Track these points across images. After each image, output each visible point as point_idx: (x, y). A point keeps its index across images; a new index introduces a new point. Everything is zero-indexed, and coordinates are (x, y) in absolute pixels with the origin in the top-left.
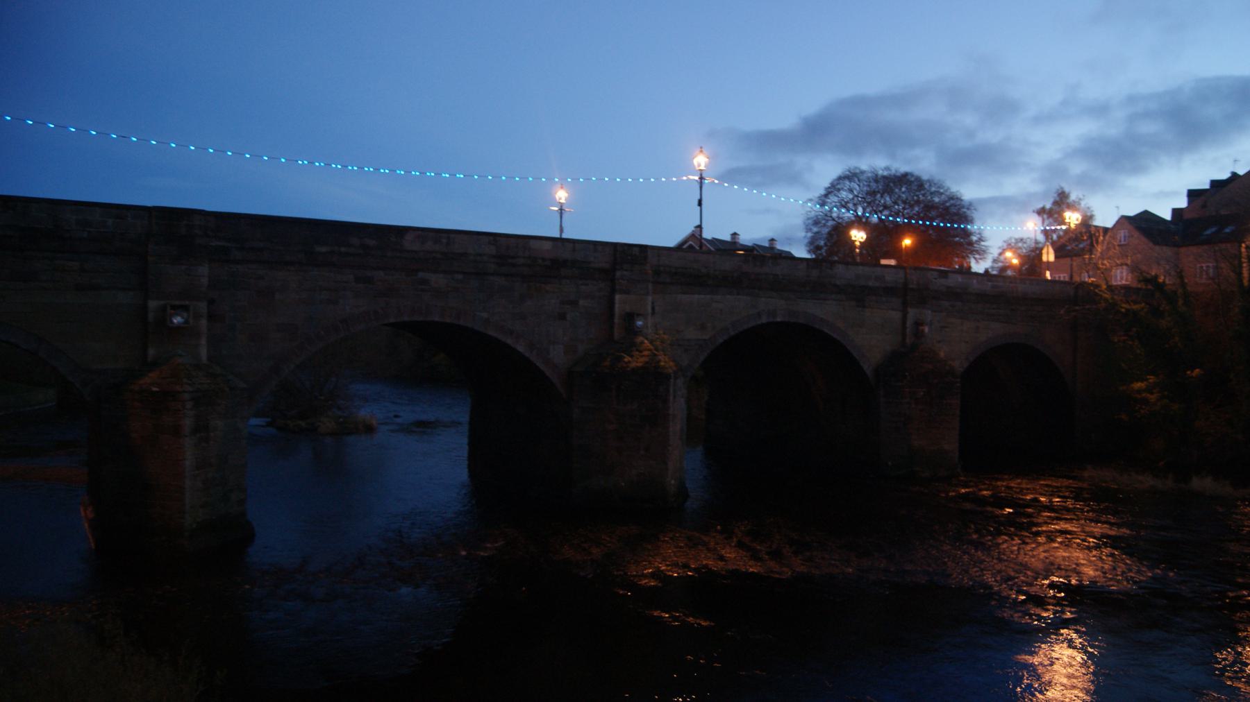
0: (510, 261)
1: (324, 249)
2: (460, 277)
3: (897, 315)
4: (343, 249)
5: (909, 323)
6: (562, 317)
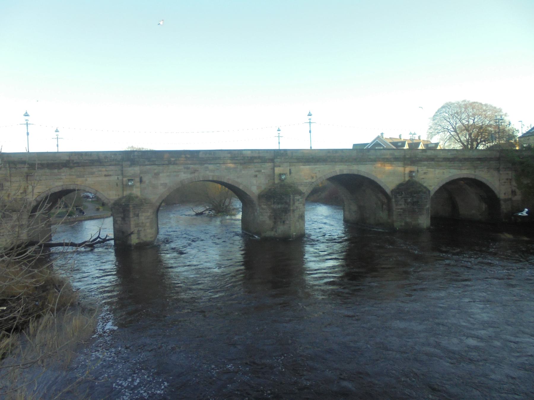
2: (219, 165)
6: (256, 176)
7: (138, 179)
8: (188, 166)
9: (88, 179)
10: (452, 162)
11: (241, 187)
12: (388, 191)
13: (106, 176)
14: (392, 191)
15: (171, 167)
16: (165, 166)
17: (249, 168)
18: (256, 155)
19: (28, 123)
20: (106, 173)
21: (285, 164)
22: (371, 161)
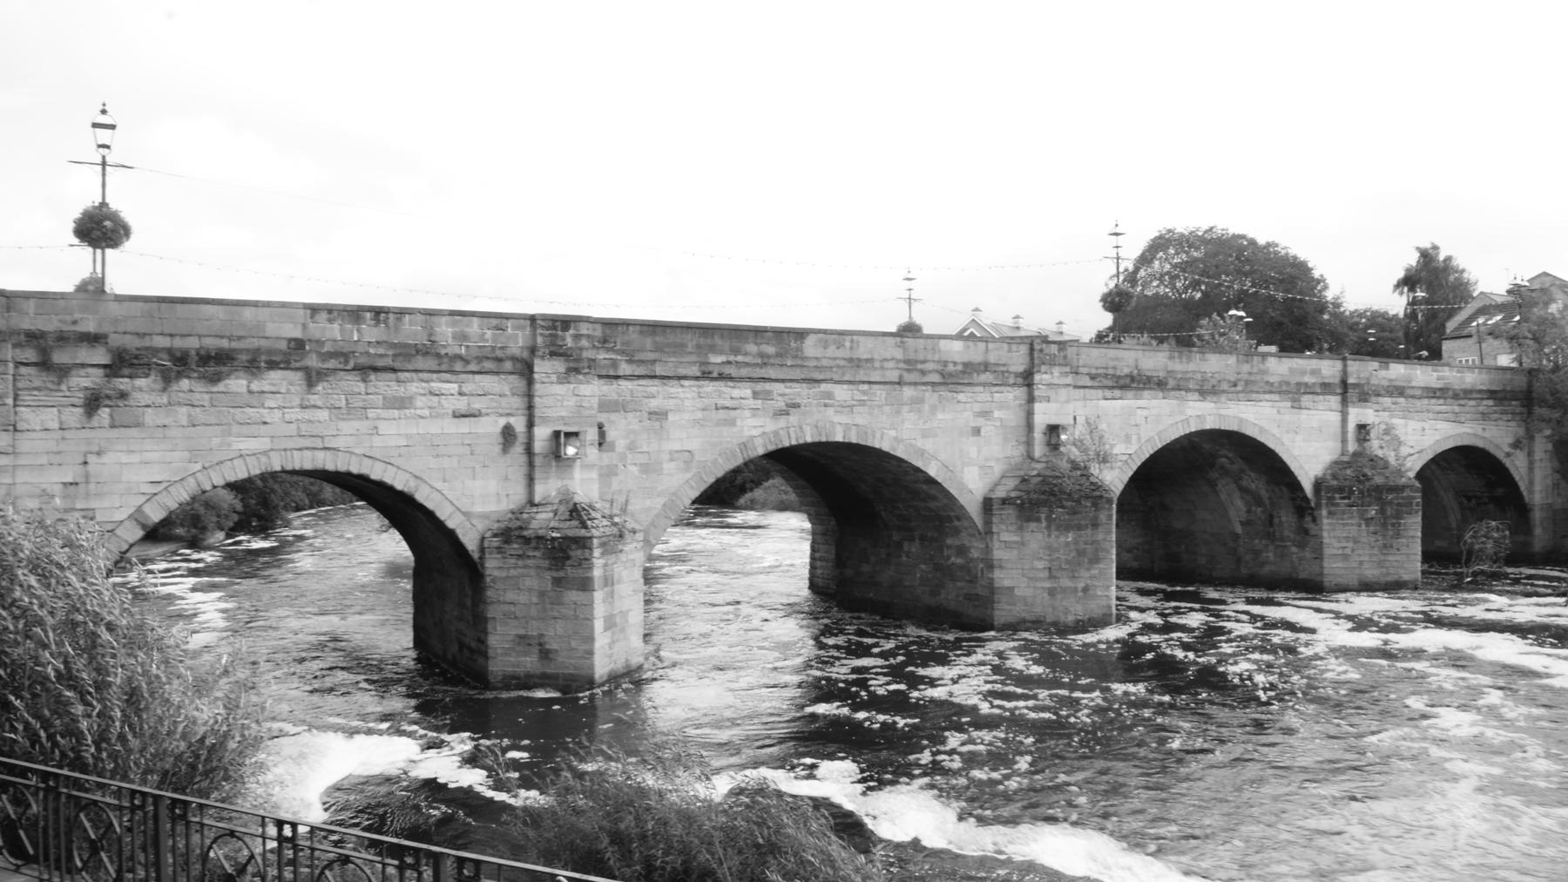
0: (920, 366)
2: (866, 387)
3: (1335, 417)
4: (740, 358)
5: (1351, 426)
6: (977, 431)
7: (592, 434)
8: (768, 386)
9: (384, 427)
10: (1441, 401)
12: (1308, 486)
13: (458, 415)
14: (1318, 485)
15: (709, 387)
16: (686, 383)
18: (976, 354)
19: (109, 160)
20: (461, 404)
21: (1063, 392)
22: (1271, 392)
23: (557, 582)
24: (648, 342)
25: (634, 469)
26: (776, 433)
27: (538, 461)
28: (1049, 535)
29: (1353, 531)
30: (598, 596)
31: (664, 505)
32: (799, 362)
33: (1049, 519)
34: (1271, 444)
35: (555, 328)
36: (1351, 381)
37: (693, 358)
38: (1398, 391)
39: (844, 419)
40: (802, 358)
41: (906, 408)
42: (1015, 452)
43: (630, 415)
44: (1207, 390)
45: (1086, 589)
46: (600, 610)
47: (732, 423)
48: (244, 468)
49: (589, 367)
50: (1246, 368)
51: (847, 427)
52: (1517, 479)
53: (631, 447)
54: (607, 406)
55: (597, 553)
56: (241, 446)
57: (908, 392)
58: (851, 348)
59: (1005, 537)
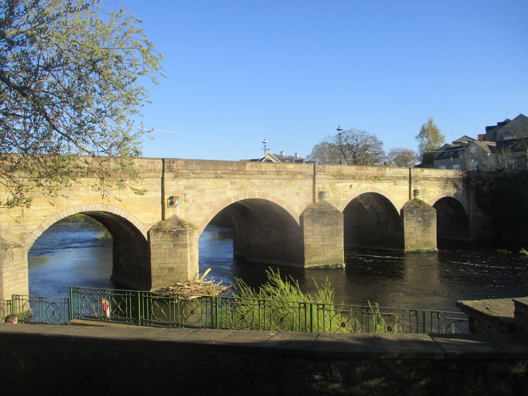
1: (219, 172)
2: (264, 180)
4: (226, 171)
6: (298, 194)
8: (235, 180)
11: (285, 207)
14: (402, 211)
16: (210, 180)
17: (293, 185)
23: (175, 245)
24: (198, 167)
25: (195, 208)
26: (237, 196)
27: (166, 206)
28: (322, 228)
29: (414, 225)
30: (189, 249)
31: (204, 220)
32: (244, 173)
33: (322, 222)
34: (387, 197)
35: (170, 163)
36: (412, 176)
37: (212, 172)
38: (426, 179)
39: (258, 191)
40: (245, 171)
41: (276, 187)
42: (310, 200)
43: (193, 191)
44: (368, 178)
45: (334, 245)
46: (189, 254)
47: (224, 193)
48: (74, 211)
49: (181, 175)
50: (380, 172)
51: (259, 194)
52: (464, 207)
53: (194, 201)
54: (187, 188)
55: (188, 236)
56: (73, 203)
57: (277, 181)
58: (260, 167)
59: (308, 228)
